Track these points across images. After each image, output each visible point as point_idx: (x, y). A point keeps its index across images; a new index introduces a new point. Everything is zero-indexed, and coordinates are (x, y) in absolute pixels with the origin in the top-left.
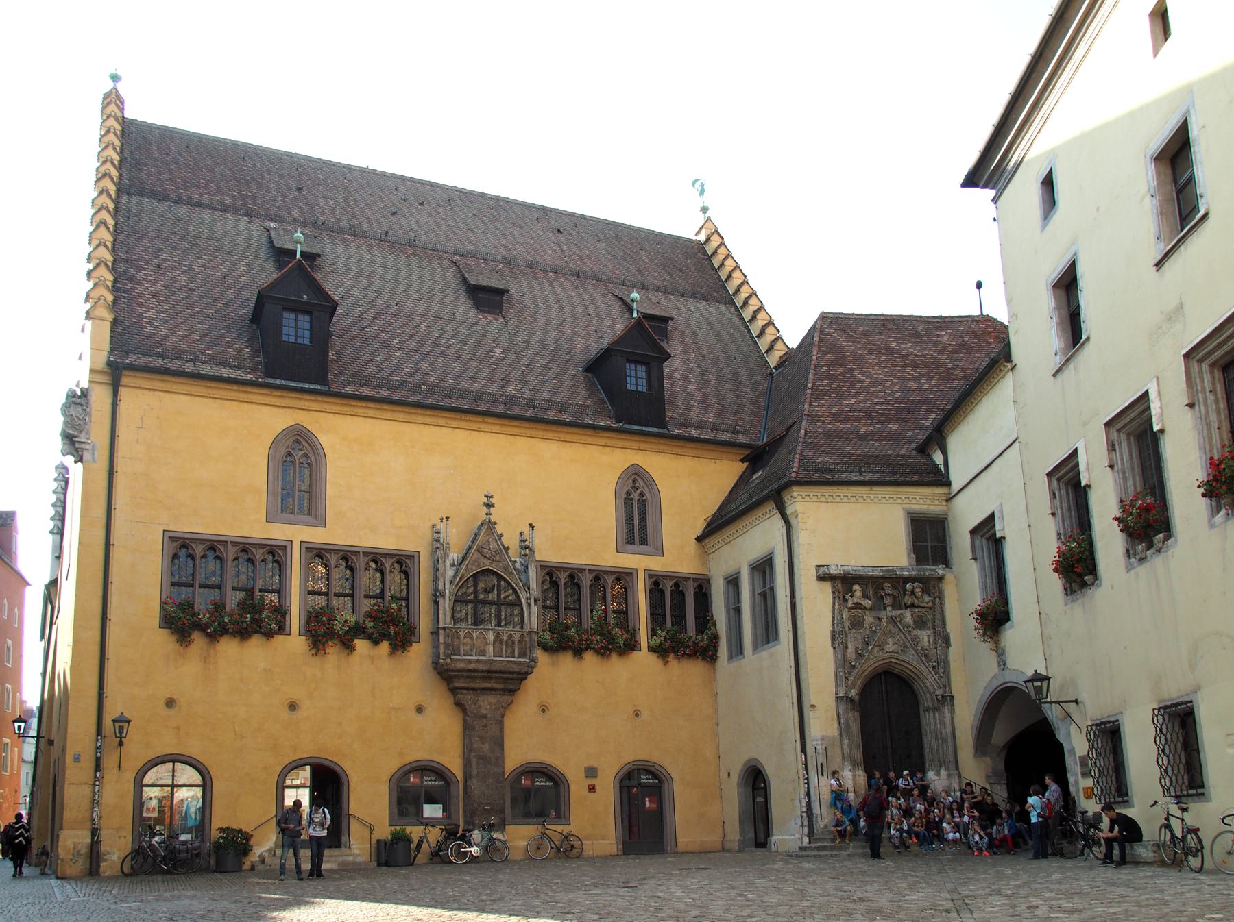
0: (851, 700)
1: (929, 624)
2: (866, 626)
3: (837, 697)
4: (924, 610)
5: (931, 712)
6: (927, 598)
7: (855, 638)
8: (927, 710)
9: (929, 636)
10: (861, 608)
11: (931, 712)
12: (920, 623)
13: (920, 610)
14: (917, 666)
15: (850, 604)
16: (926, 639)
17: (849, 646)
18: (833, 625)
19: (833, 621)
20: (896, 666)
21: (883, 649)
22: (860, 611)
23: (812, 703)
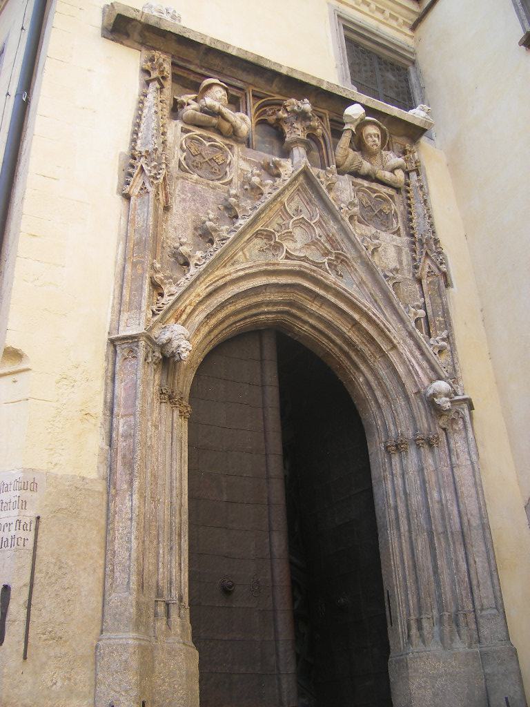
0: (167, 361)
1: (399, 224)
2: (232, 175)
3: (112, 342)
4: (384, 190)
5: (412, 451)
6: (393, 159)
7: (194, 192)
8: (399, 447)
9: (399, 250)
10: (218, 130)
11: (412, 451)
12: (376, 215)
13: (375, 186)
14: (372, 310)
15: (191, 109)
16: (392, 253)
17: (176, 207)
18: (134, 141)
19: (136, 133)
20: (314, 307)
21: (278, 247)
22: (219, 141)
23: (12, 341)
